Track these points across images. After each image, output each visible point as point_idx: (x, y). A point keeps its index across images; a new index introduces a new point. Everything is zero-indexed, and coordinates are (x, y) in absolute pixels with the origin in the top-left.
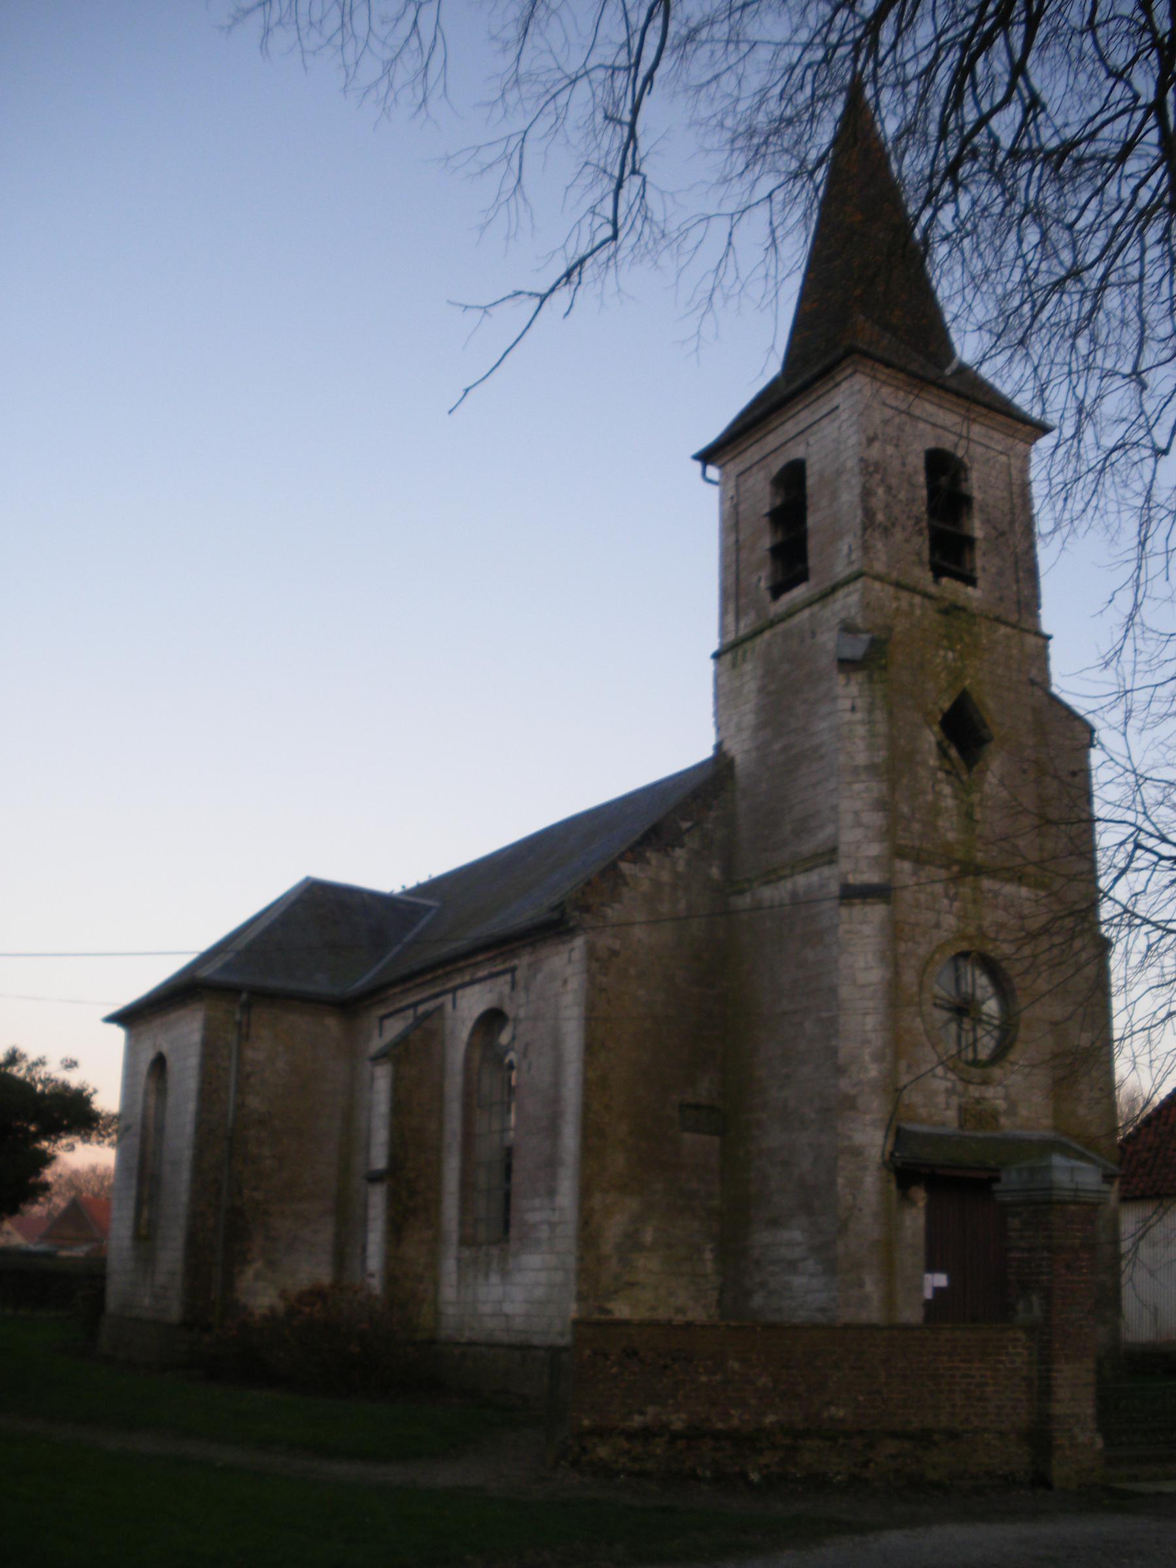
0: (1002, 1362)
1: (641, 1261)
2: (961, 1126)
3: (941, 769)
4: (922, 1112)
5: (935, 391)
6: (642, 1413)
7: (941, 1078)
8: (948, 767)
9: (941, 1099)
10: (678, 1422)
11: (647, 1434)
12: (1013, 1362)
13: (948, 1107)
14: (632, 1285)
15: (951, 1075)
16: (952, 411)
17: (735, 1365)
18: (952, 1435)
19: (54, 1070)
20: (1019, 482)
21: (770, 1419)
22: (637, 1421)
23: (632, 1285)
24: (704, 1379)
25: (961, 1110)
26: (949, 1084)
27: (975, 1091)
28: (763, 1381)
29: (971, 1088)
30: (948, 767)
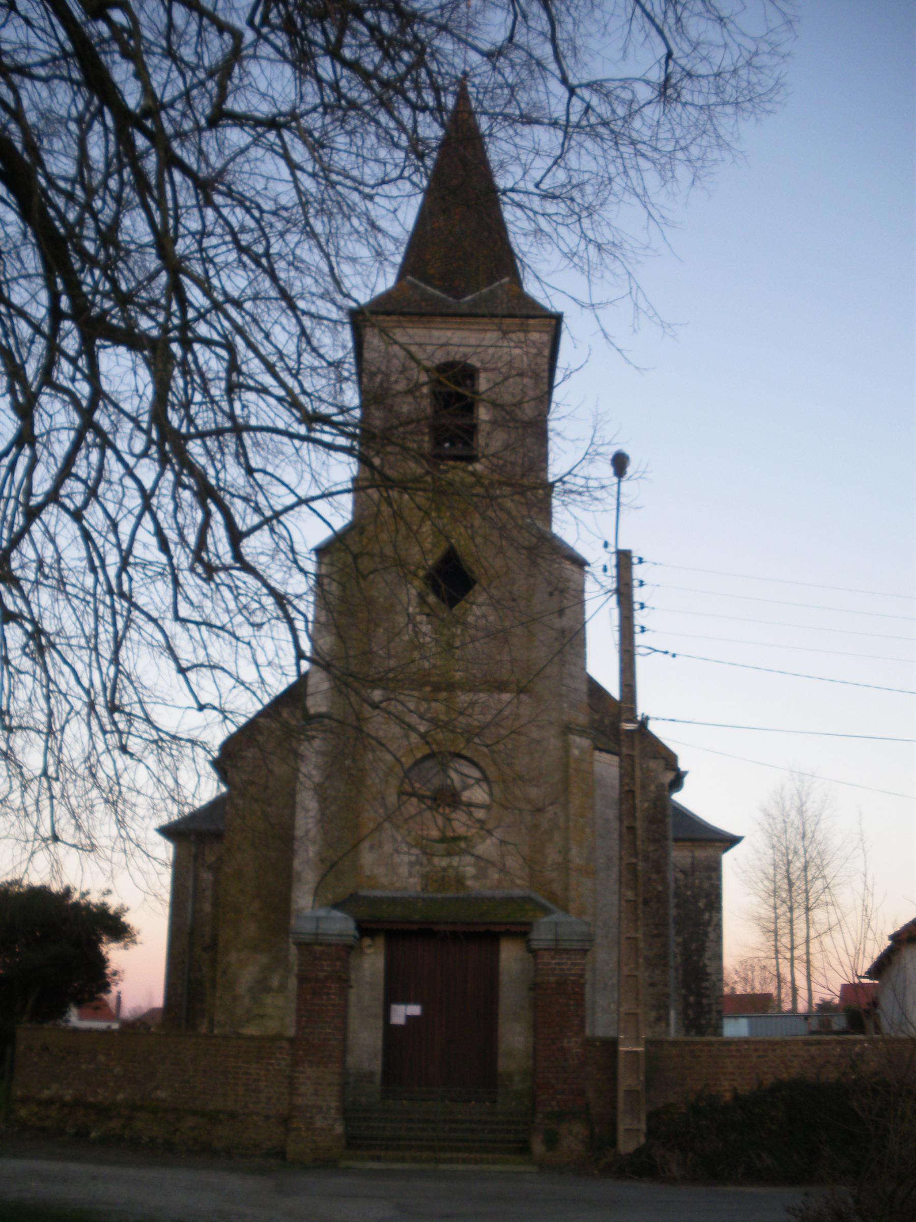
0: (272, 1064)
1: (268, 999)
2: (423, 890)
3: (421, 613)
4: (385, 881)
5: (438, 319)
6: (48, 1088)
7: (405, 853)
8: (427, 610)
9: (404, 871)
10: (68, 1095)
11: (50, 1102)
12: (279, 1065)
13: (410, 875)
14: (262, 1016)
15: (415, 851)
16: (459, 329)
17: (102, 1058)
18: (233, 1115)
19: (95, 898)
20: (437, 375)
21: (120, 1096)
22: (46, 1094)
23: (262, 1016)
24: (84, 1067)
25: (425, 877)
26: (413, 858)
27: (441, 862)
28: (118, 1070)
29: (436, 860)
30: (427, 610)
